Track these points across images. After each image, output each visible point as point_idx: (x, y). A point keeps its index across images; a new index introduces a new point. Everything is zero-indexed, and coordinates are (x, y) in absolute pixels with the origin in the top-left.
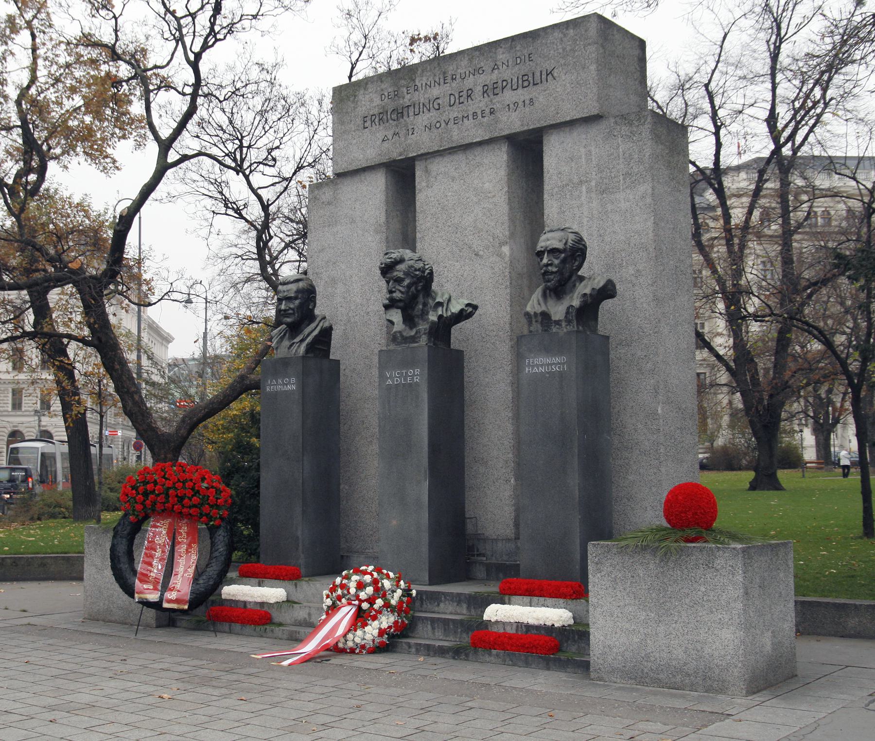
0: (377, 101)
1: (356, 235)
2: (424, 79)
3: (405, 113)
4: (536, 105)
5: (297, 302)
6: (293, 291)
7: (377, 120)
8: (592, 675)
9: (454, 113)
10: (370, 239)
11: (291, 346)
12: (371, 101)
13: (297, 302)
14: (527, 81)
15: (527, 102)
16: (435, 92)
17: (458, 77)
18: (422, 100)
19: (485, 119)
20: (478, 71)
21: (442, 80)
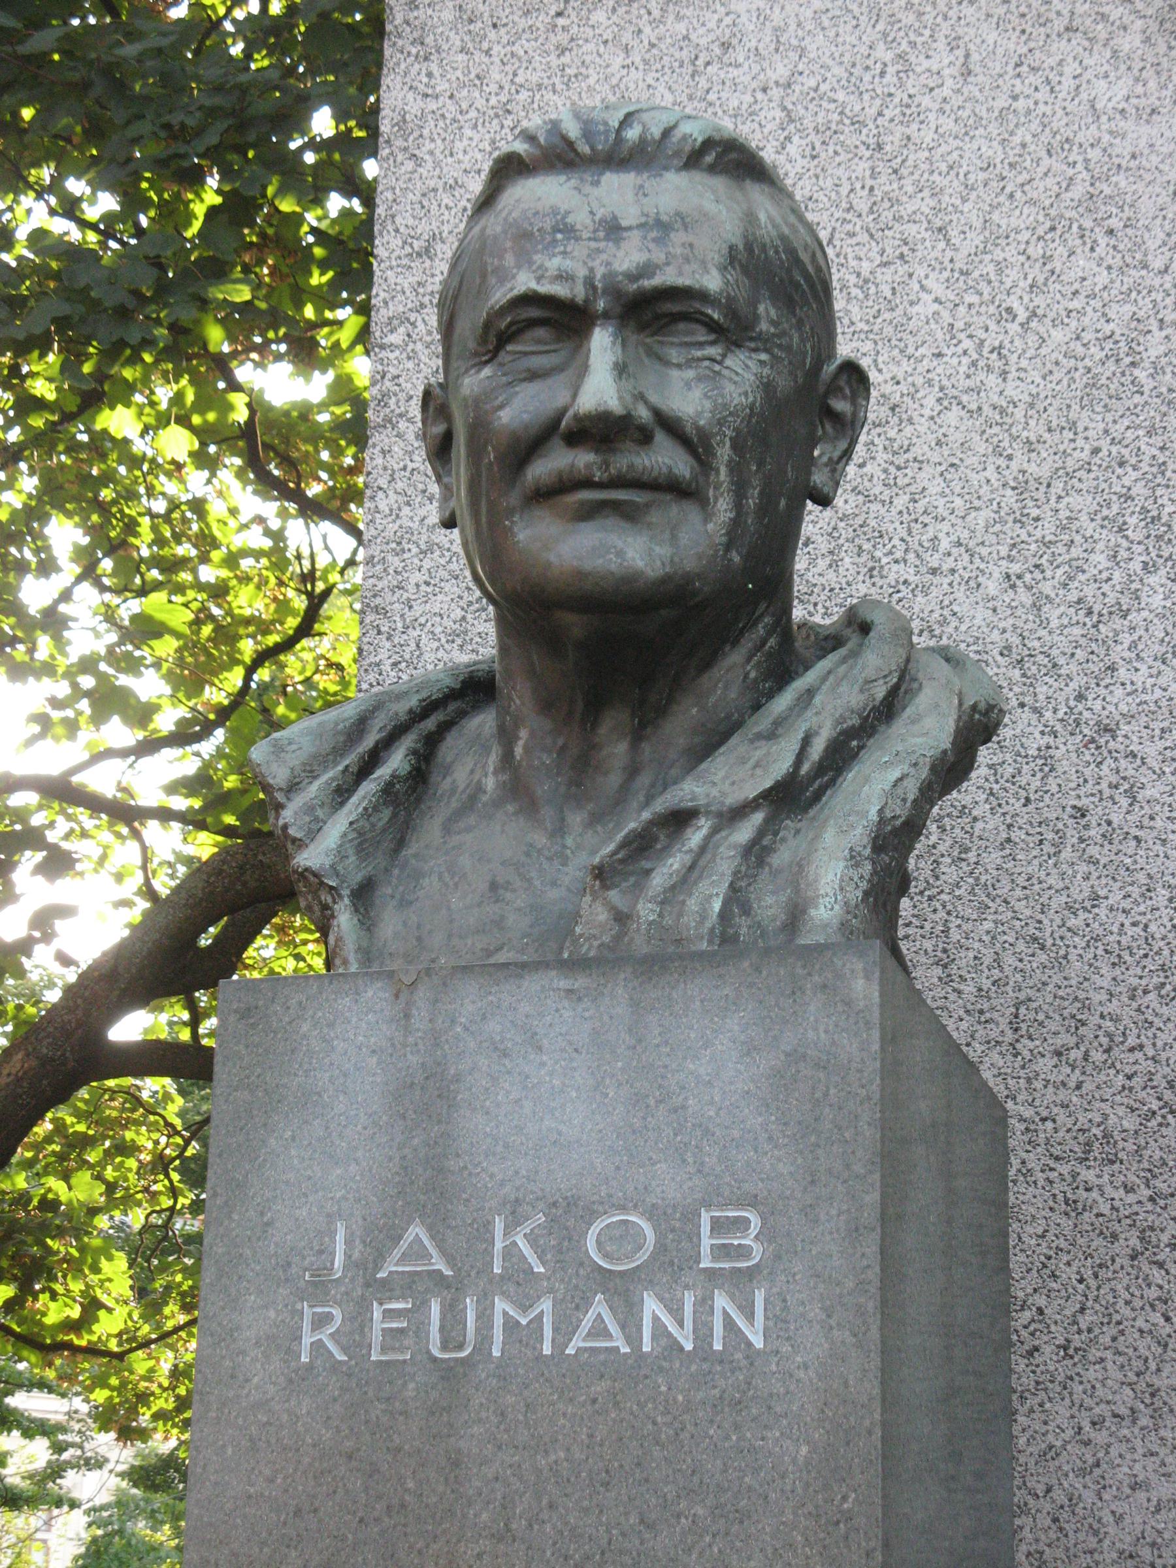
1: (943, 59)
5: (742, 377)
6: (711, 248)
10: (1112, 92)
11: (642, 847)
13: (742, 377)
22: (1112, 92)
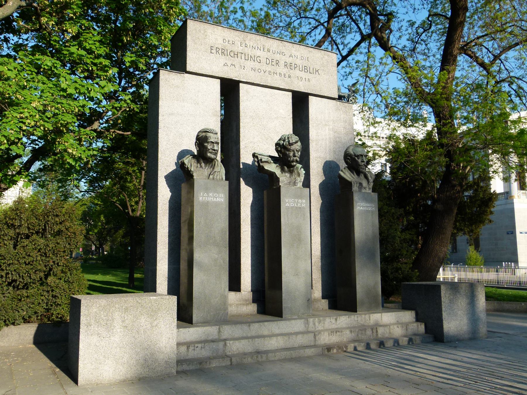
0: (220, 41)
2: (251, 43)
3: (239, 55)
4: (311, 82)
7: (220, 52)
8: (445, 341)
9: (269, 68)
12: (216, 39)
14: (306, 69)
15: (307, 79)
16: (258, 53)
17: (271, 51)
18: (250, 54)
19: (286, 79)
20: (283, 54)
21: (262, 49)
22: (209, 117)
